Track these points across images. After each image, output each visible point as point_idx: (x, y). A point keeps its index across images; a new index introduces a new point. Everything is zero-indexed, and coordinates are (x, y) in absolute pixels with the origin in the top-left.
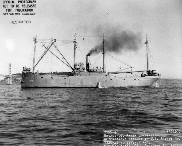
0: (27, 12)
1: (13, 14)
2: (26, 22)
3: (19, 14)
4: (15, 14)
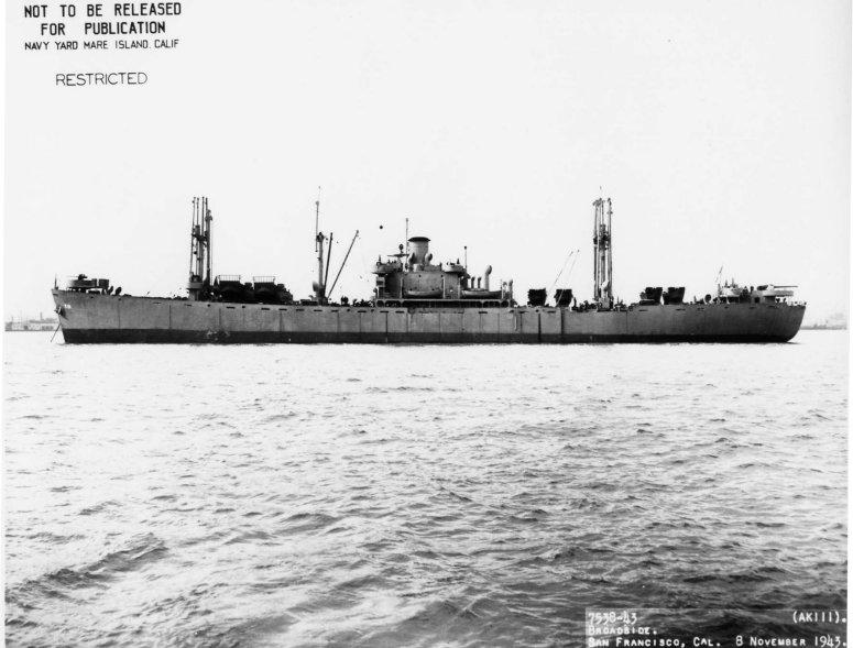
2: (125, 76)
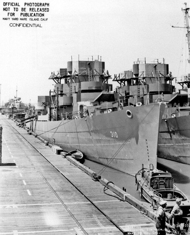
0: (36, 17)
1: (16, 19)
3: (26, 19)
4: (19, 19)
